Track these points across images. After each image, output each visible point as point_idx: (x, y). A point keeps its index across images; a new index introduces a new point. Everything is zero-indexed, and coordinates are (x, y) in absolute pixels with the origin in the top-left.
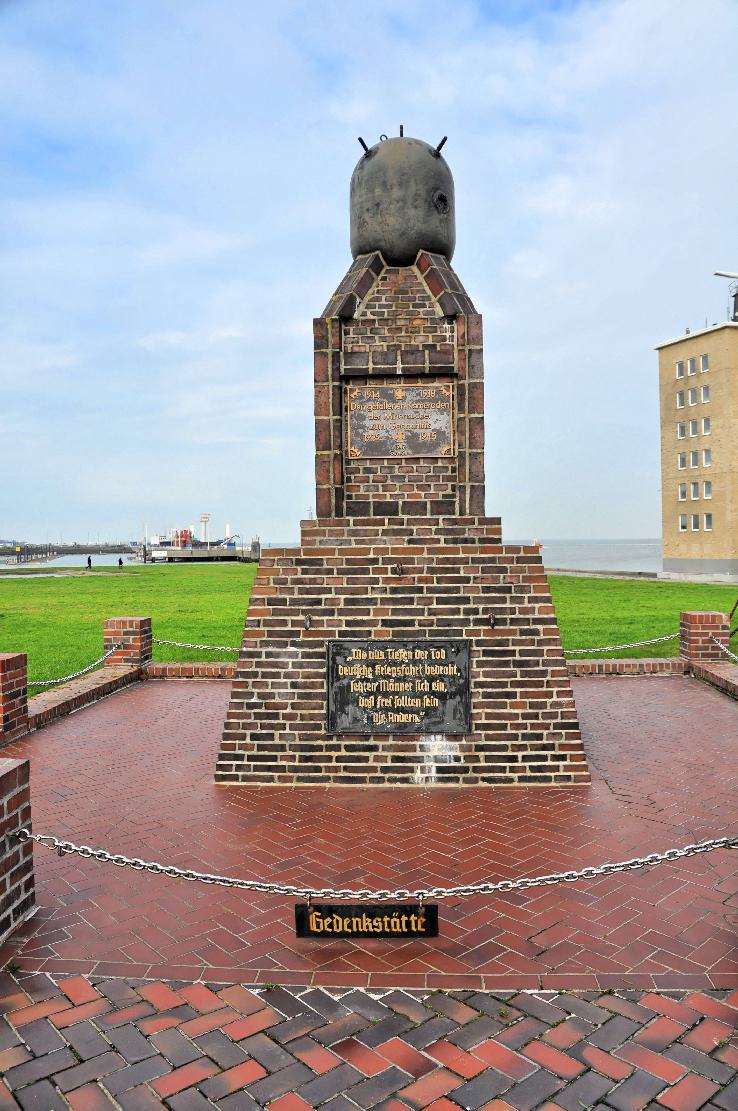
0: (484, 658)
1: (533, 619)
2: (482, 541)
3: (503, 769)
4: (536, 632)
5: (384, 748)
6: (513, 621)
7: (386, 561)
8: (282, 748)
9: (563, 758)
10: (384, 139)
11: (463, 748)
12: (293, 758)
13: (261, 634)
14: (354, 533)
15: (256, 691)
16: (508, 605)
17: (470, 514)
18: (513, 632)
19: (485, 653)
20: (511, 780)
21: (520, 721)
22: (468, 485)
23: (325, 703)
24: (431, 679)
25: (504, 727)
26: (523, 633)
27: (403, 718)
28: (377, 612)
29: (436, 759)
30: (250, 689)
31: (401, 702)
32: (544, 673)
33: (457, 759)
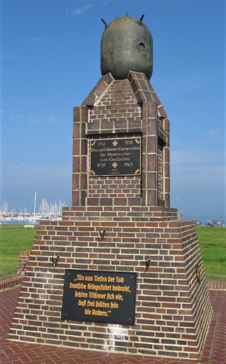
0: (144, 284)
1: (172, 263)
3: (150, 346)
4: (173, 271)
5: (90, 329)
6: (161, 264)
7: (98, 229)
8: (40, 324)
9: (184, 343)
11: (130, 332)
12: (44, 330)
13: (35, 264)
18: (160, 270)
20: (155, 353)
21: (162, 320)
24: (116, 293)
25: (152, 322)
27: (100, 313)
28: (91, 256)
29: (116, 337)
30: (28, 292)
31: (99, 304)
32: (176, 294)
33: (126, 338)
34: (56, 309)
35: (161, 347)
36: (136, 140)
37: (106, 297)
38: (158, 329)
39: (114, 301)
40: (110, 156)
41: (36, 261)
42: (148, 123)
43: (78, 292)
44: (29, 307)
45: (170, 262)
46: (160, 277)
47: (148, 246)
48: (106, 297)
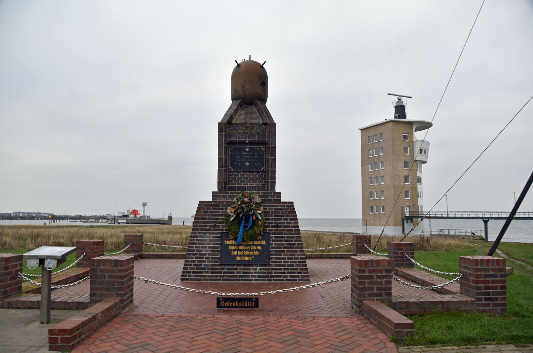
0: (275, 239)
1: (291, 226)
2: (274, 200)
3: (280, 276)
4: (292, 230)
5: (240, 269)
6: (285, 227)
8: (204, 269)
9: (301, 273)
10: (244, 60)
12: (208, 272)
13: (198, 230)
14: (230, 196)
15: (196, 249)
16: (283, 221)
17: (271, 191)
18: (284, 230)
19: (275, 237)
21: (286, 260)
22: (270, 181)
23: (220, 253)
24: (257, 245)
25: (281, 262)
26: (287, 230)
27: (247, 258)
30: (194, 249)
31: (245, 253)
32: (294, 244)
34: (215, 258)
35: (287, 276)
36: (262, 148)
37: (250, 248)
38: (285, 266)
39: (256, 250)
40: (244, 158)
41: (198, 228)
42: (271, 137)
43: (231, 246)
44: (195, 259)
45: (290, 225)
46: (284, 234)
47: (276, 216)
48: (250, 248)
